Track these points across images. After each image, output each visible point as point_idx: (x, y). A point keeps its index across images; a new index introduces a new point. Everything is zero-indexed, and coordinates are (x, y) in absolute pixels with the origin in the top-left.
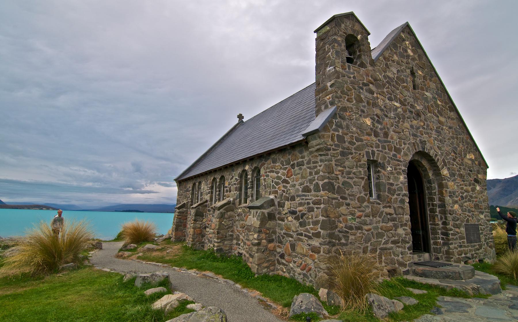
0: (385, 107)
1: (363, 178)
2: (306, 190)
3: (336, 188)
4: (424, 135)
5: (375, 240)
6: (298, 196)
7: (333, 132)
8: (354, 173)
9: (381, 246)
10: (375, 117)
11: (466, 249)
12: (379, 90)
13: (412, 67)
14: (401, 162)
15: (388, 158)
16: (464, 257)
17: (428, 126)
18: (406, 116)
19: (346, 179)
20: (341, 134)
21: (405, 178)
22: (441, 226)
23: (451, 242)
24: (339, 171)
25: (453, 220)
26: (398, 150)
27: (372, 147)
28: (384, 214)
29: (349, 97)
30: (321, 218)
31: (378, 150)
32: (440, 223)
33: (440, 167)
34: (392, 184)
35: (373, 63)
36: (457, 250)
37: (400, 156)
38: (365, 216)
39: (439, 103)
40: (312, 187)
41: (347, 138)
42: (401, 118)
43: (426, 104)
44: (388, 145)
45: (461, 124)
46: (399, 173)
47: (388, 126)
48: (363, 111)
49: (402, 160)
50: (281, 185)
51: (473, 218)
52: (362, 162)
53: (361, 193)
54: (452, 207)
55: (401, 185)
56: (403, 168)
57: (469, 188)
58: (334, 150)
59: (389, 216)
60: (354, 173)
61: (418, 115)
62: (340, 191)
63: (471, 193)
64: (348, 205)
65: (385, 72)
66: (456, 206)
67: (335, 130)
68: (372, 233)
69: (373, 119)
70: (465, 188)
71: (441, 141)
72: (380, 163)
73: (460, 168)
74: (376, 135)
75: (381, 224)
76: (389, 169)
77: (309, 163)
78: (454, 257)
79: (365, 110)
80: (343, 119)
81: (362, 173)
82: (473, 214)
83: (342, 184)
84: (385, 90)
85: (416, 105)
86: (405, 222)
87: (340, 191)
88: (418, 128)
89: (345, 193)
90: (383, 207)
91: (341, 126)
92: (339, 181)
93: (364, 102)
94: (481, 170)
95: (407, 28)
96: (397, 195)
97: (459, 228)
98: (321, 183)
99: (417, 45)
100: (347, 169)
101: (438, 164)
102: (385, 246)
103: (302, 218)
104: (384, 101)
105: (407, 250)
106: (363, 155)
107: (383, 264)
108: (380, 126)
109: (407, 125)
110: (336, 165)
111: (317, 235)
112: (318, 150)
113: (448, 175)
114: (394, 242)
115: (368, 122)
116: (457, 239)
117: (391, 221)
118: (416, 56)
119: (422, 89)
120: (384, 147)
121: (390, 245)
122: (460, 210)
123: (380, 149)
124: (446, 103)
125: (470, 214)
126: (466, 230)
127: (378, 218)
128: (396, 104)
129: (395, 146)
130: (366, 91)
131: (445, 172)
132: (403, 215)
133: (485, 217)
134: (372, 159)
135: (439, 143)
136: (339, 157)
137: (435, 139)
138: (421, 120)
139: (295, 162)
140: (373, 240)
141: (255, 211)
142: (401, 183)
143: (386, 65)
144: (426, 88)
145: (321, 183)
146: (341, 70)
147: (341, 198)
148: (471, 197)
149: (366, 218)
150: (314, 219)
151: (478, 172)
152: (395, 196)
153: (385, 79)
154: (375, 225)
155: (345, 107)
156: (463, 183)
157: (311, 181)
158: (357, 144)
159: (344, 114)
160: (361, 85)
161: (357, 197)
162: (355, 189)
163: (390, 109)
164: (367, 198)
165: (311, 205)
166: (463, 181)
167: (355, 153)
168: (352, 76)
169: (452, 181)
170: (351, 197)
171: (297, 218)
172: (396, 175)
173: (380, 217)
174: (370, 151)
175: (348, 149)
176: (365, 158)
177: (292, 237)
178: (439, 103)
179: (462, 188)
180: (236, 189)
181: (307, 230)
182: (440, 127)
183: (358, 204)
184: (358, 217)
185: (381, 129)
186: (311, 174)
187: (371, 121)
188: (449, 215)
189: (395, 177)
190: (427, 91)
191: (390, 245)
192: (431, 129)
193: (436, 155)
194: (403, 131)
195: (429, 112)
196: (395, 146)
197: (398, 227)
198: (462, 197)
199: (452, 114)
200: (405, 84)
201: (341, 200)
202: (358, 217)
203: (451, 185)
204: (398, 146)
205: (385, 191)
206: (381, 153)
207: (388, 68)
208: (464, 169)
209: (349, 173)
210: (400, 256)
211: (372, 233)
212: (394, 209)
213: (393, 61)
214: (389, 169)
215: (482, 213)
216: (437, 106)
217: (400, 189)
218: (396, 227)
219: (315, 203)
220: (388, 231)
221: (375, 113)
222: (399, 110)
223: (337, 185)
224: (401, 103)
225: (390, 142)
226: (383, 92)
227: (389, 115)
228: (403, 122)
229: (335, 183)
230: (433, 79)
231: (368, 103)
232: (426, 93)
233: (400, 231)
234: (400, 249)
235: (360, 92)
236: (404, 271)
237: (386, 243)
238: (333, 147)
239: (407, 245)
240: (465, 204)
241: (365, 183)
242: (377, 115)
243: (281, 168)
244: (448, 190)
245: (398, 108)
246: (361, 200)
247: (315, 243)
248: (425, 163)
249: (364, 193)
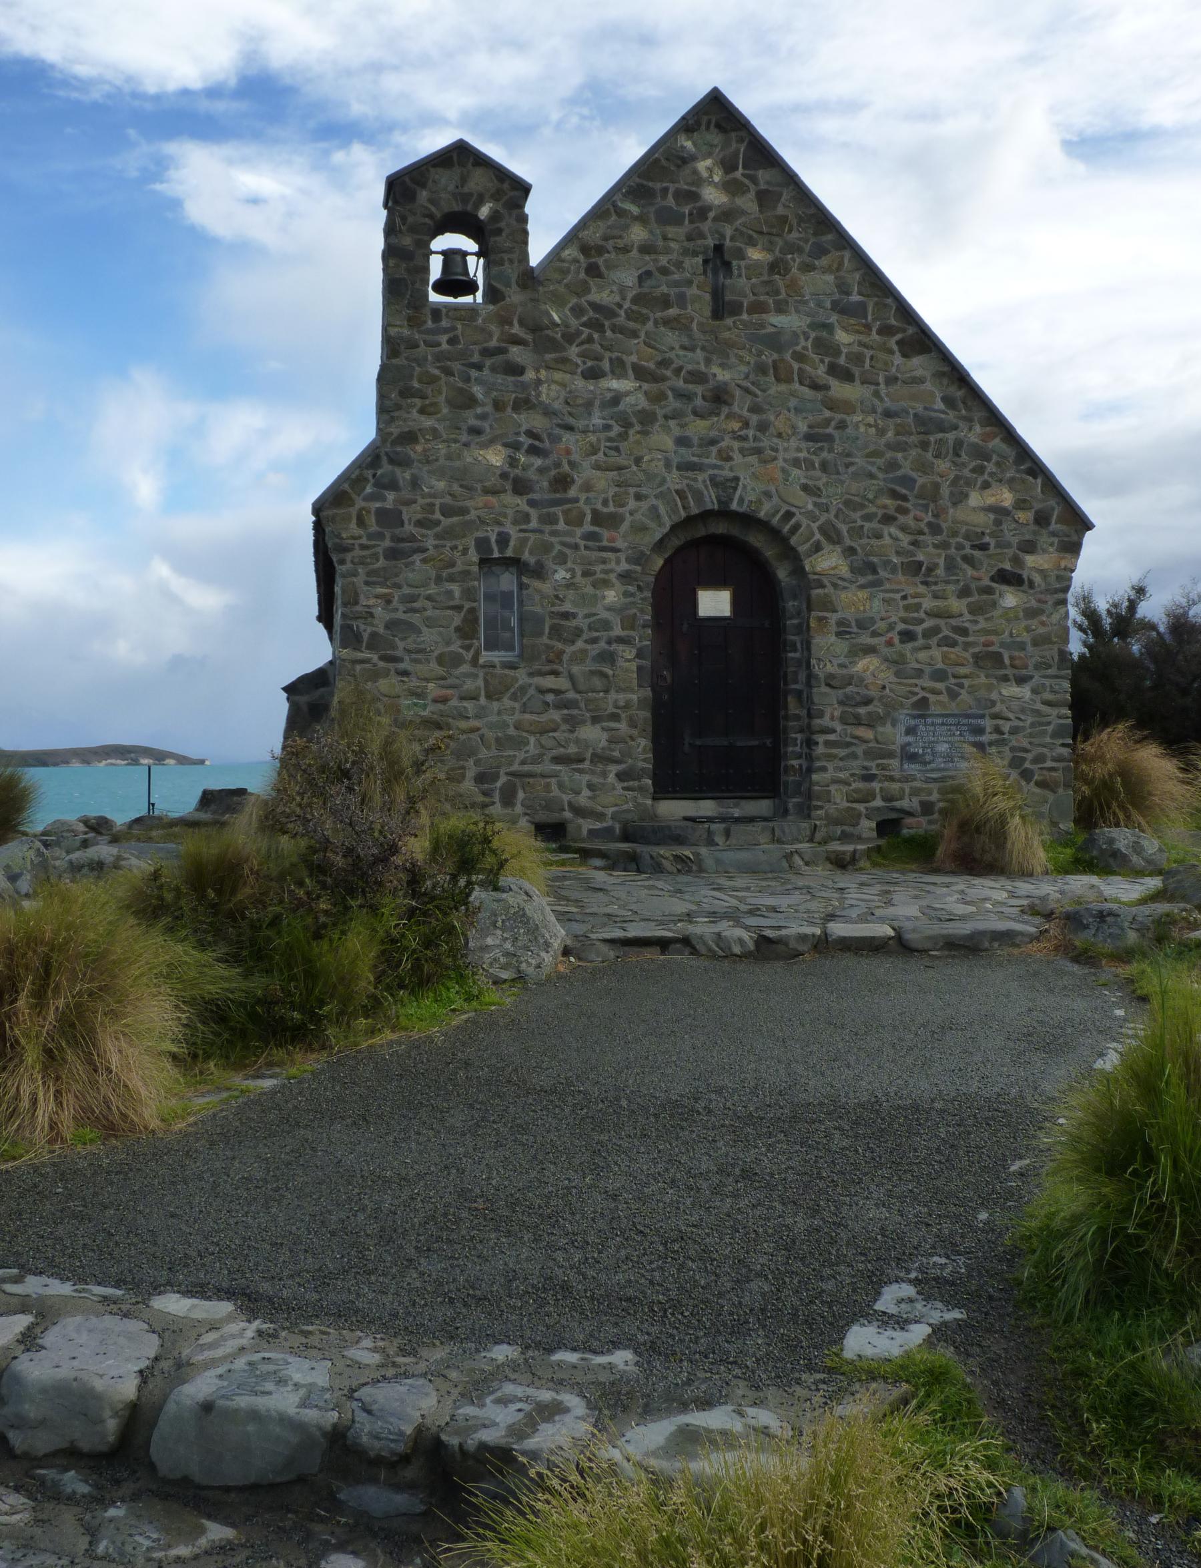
0: (567, 403)
1: (458, 608)
3: (366, 636)
4: (738, 459)
5: (494, 752)
7: (363, 504)
8: (429, 598)
9: (515, 767)
10: (522, 438)
11: (895, 786)
12: (548, 357)
13: (719, 249)
14: (615, 550)
15: (558, 547)
16: (878, 809)
17: (763, 427)
18: (660, 413)
19: (400, 615)
20: (389, 504)
21: (626, 594)
22: (806, 721)
23: (818, 764)
24: (377, 597)
25: (841, 703)
26: (613, 521)
27: (499, 523)
28: (532, 691)
29: (427, 402)
31: (521, 531)
32: (804, 713)
33: (802, 549)
34: (566, 616)
35: (529, 278)
36: (845, 789)
37: (620, 538)
38: (462, 698)
41: (409, 514)
43: (769, 357)
44: (565, 513)
45: (960, 394)
46: (606, 584)
47: (575, 457)
48: (475, 431)
49: (620, 544)
51: (953, 695)
52: (460, 567)
53: (448, 643)
54: (841, 666)
55: (605, 615)
56: (624, 566)
57: (957, 605)
58: (363, 547)
59: (550, 697)
60: (429, 598)
61: (719, 398)
62: (375, 642)
63: (967, 617)
64: (405, 673)
65: (587, 290)
66: (866, 665)
67: (371, 498)
68: (482, 737)
69: (516, 446)
70: (928, 604)
71: (824, 467)
72: (526, 564)
73: (914, 543)
74: (520, 487)
75: (517, 716)
78: (827, 806)
79: (486, 425)
80: (400, 464)
81: (457, 594)
82: (961, 686)
83: (387, 627)
84: (573, 351)
85: (715, 369)
86: (611, 709)
87: (375, 642)
88: (713, 442)
89: (394, 648)
90: (531, 675)
91: (393, 485)
92: (376, 622)
93: (483, 405)
94: (1044, 539)
95: (715, 115)
96: (586, 641)
97: (870, 726)
99: (762, 154)
100: (406, 590)
101: (793, 541)
102: (526, 768)
104: (563, 385)
105: (611, 778)
106: (465, 551)
107: (519, 809)
108: (538, 462)
110: (367, 583)
113: (844, 570)
114: (557, 760)
116: (854, 756)
117: (558, 706)
118: (748, 203)
119: (758, 308)
120: (551, 520)
121: (548, 767)
122: (887, 676)
123: (534, 524)
124: (886, 331)
125: (940, 686)
127: (507, 702)
128: (615, 384)
129: (595, 513)
130: (493, 369)
131: (829, 562)
132: (607, 691)
133: (1035, 691)
134: (496, 555)
135: (818, 473)
136: (382, 563)
137: (796, 463)
138: (729, 416)
140: (483, 753)
142: (609, 609)
143: (593, 271)
144: (777, 303)
146: (406, 332)
147: (382, 658)
148: (964, 632)
149: (466, 704)
151: (1029, 547)
152: (580, 644)
153: (577, 317)
154: (493, 718)
155: (410, 432)
156: (922, 589)
158: (446, 522)
159: (408, 449)
160: (476, 358)
161: (436, 654)
162: (428, 636)
163: (589, 405)
164: (468, 656)
166: (925, 583)
167: (436, 547)
168: (444, 339)
169: (862, 587)
170: (414, 656)
172: (589, 590)
173: (514, 698)
174: (493, 539)
175: (412, 538)
176: (473, 556)
179: (918, 607)
182: (828, 422)
183: (440, 671)
184: (435, 701)
185: (541, 470)
187: (504, 452)
188: (824, 689)
189: (583, 597)
190: (781, 309)
191: (548, 767)
192: (780, 435)
193: (789, 515)
194: (638, 461)
195: (778, 380)
196: (595, 513)
197: (583, 722)
199: (919, 365)
200: (673, 312)
201: (382, 664)
202: (435, 701)
203: (853, 601)
204: (611, 508)
205: (541, 634)
206: (533, 537)
207: (600, 275)
208: (945, 545)
209: (412, 599)
210: (586, 792)
211: (482, 737)
212: (571, 677)
213: (625, 250)
214: (561, 575)
215: (1021, 681)
216: (826, 347)
217: (606, 625)
218: (573, 723)
220: (541, 733)
221: (523, 429)
222: (630, 400)
223: (369, 629)
224: (641, 374)
225: (576, 500)
226: (565, 360)
227: (580, 424)
228: (644, 433)
229: (362, 627)
230: (824, 261)
231: (498, 406)
232: (778, 320)
233: (593, 734)
234: (587, 777)
235: (468, 379)
236: (590, 831)
237: (536, 760)
238: (364, 541)
239: (613, 769)
240: (922, 655)
241: (465, 620)
242: (530, 434)
244: (833, 618)
245: (627, 393)
246: (450, 661)
248: (756, 540)
249: (459, 643)
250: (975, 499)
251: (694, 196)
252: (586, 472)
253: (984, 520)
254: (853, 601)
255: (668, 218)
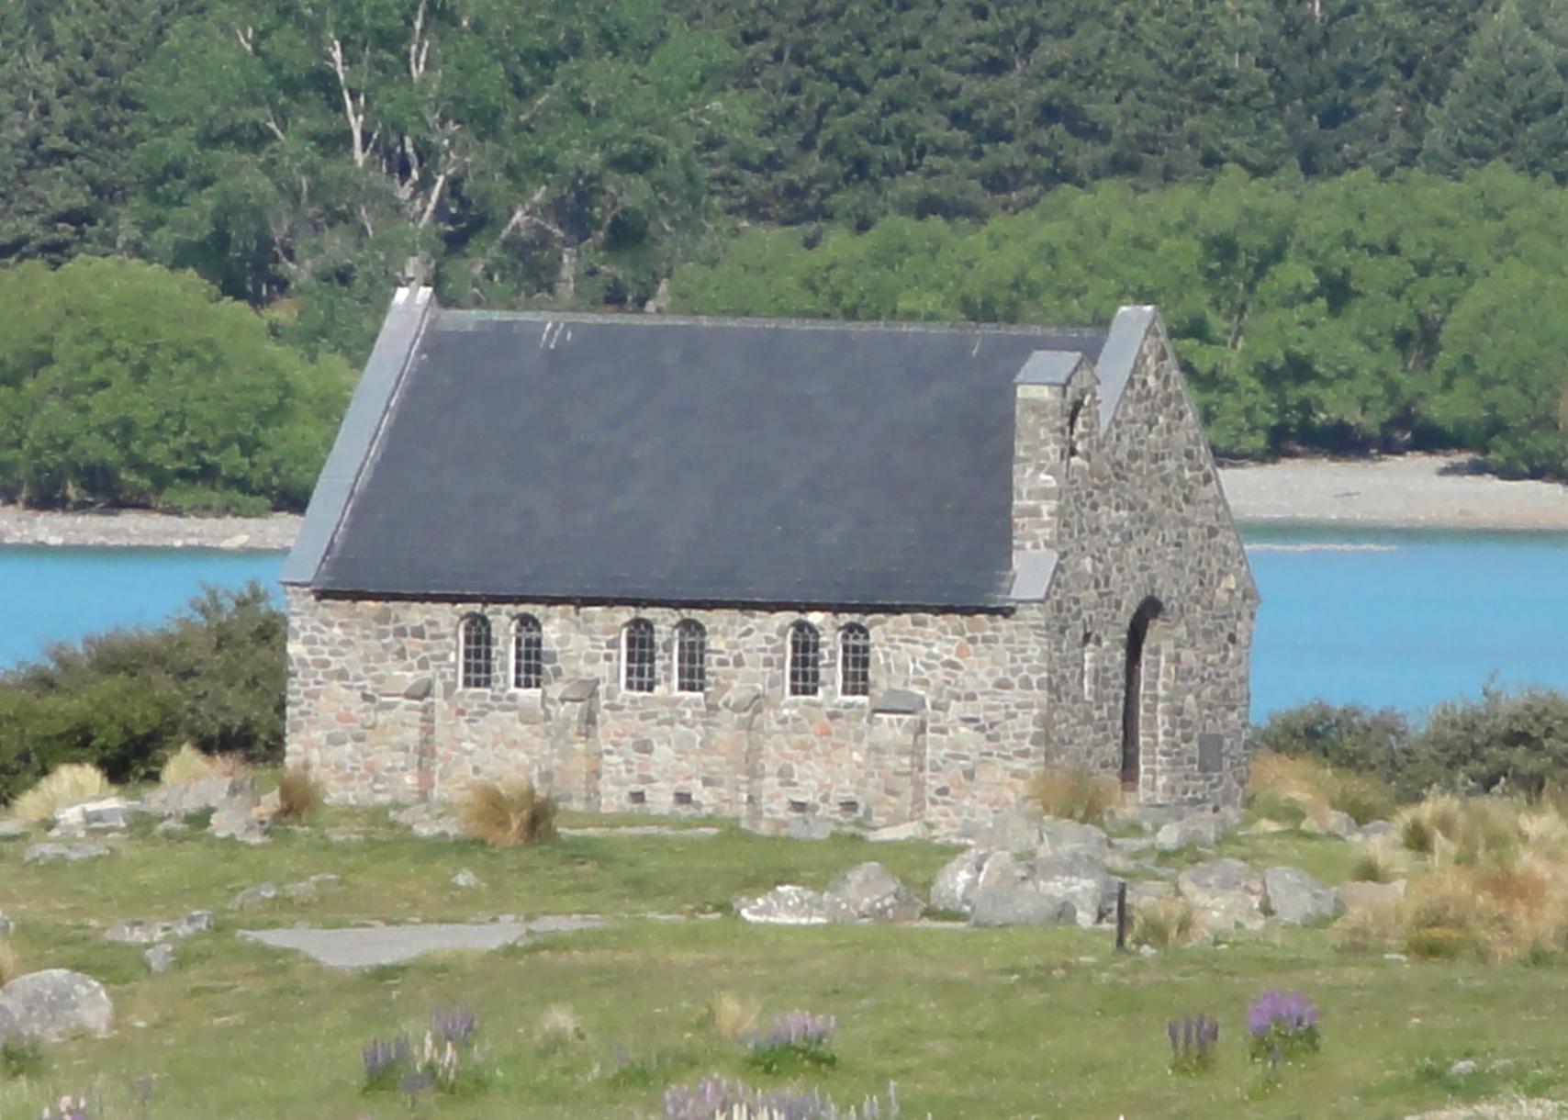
2: (1003, 685)
6: (983, 694)
30: (1032, 729)
39: (1187, 474)
40: (1015, 681)
42: (1128, 538)
50: (940, 672)
76: (1105, 643)
77: (1009, 640)
98: (1034, 679)
103: (992, 726)
109: (1132, 551)
111: (1024, 754)
112: (1034, 627)
115: (1087, 563)
126: (1201, 745)
139: (979, 635)
141: (894, 717)
145: (1034, 679)
150: (1018, 730)
151: (1239, 617)
157: (1014, 672)
165: (1013, 709)
171: (981, 729)
177: (966, 758)
178: (1187, 474)
180: (768, 663)
181: (1003, 748)
186: (1013, 660)
198: (1203, 679)
216: (1182, 483)
219: (1018, 706)
224: (1132, 508)
243: (939, 638)
247: (1020, 764)
250: (1223, 585)
251: (1144, 383)
252: (1114, 574)
253: (1225, 597)
254: (1188, 655)
255: (1139, 399)
